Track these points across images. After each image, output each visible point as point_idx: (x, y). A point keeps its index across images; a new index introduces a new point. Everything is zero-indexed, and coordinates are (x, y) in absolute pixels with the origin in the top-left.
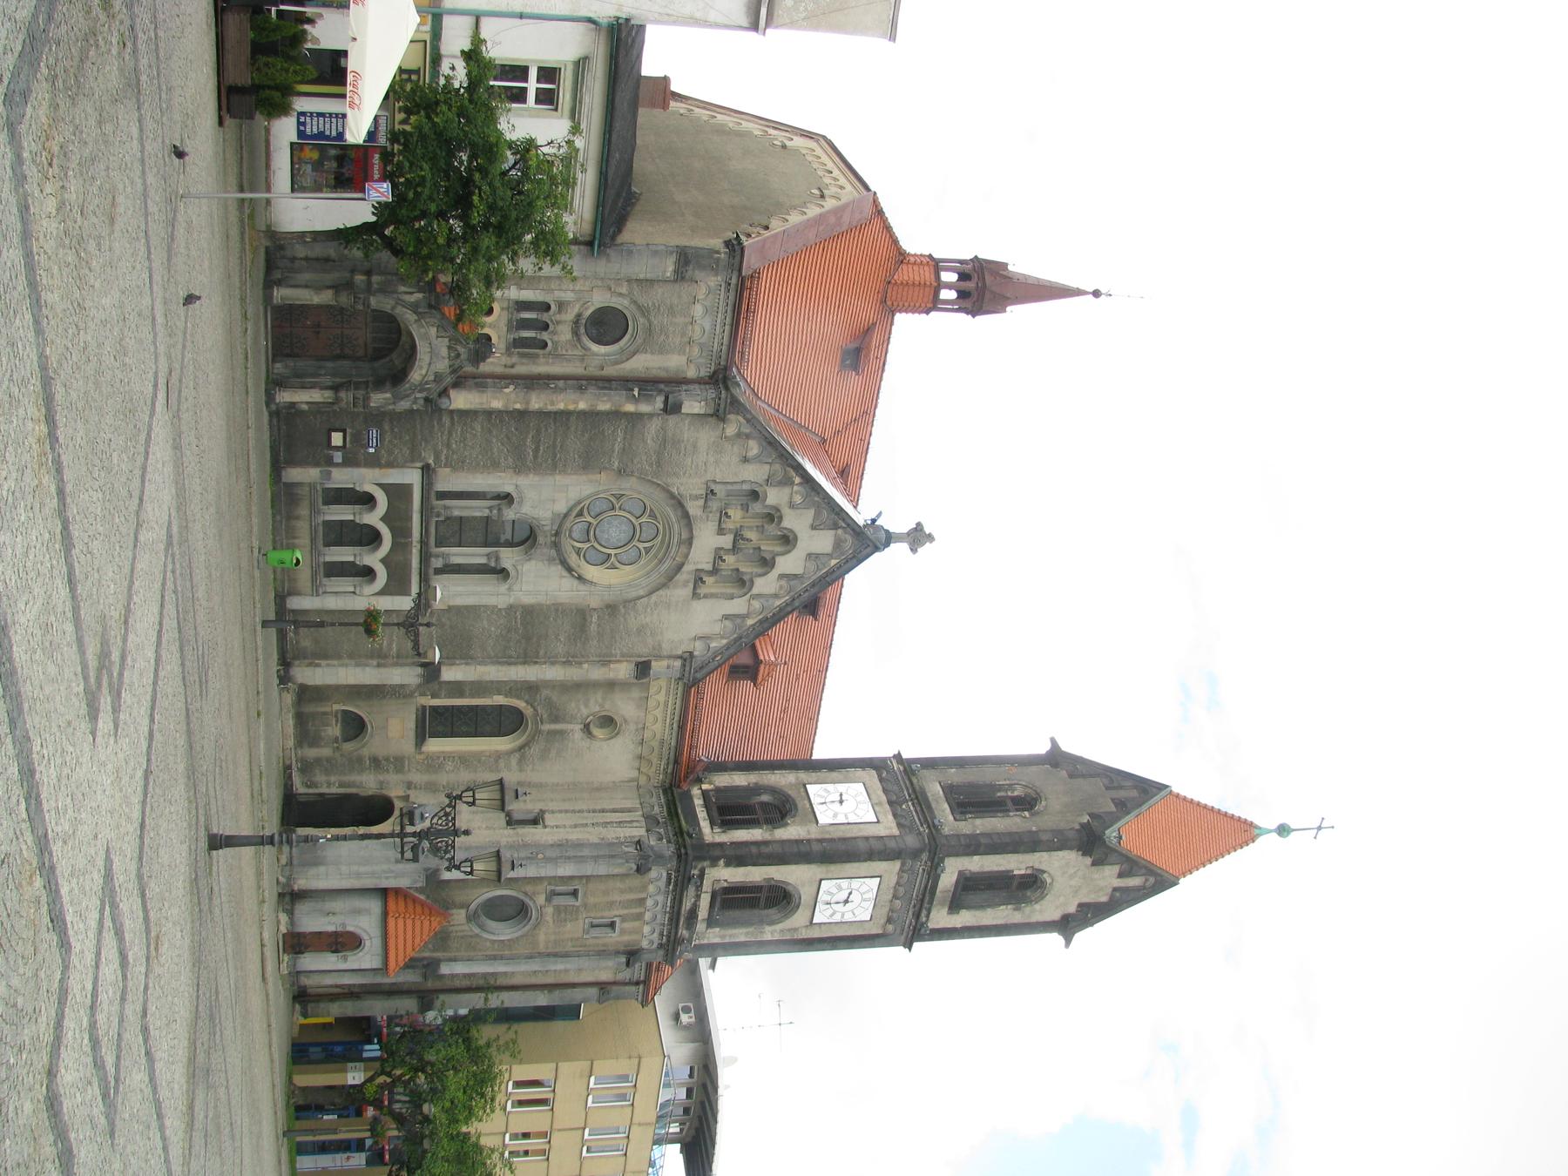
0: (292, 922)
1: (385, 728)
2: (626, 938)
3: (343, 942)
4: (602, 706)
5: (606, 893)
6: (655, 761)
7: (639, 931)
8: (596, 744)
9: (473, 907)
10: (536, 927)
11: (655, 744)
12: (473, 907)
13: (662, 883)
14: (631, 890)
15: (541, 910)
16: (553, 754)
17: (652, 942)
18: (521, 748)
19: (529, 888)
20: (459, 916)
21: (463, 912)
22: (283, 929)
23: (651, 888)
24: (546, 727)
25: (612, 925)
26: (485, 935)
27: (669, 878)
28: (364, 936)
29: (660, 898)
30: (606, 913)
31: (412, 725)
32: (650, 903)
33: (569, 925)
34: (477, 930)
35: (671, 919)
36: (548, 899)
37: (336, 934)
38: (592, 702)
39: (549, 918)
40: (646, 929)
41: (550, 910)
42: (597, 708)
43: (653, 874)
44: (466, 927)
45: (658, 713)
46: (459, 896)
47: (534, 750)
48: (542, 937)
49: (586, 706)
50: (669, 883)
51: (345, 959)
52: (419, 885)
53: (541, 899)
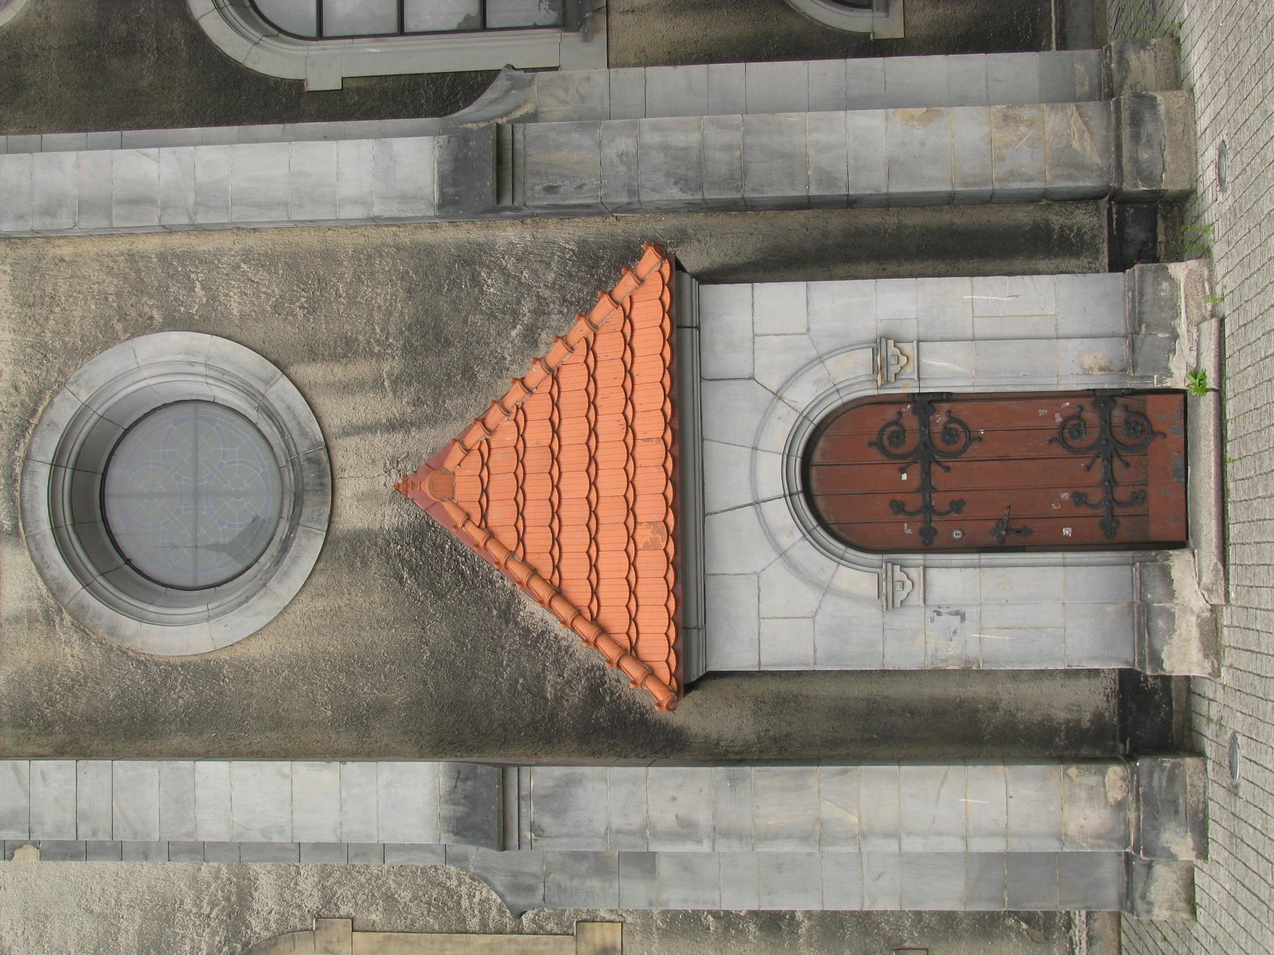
0: (1144, 620)
3: (895, 474)
12: (309, 548)
19: (70, 653)
20: (365, 497)
21: (353, 516)
22: (1190, 576)
28: (779, 514)
34: (283, 393)
37: (929, 543)
44: (338, 411)
46: (370, 614)
51: (883, 347)
52: (540, 778)
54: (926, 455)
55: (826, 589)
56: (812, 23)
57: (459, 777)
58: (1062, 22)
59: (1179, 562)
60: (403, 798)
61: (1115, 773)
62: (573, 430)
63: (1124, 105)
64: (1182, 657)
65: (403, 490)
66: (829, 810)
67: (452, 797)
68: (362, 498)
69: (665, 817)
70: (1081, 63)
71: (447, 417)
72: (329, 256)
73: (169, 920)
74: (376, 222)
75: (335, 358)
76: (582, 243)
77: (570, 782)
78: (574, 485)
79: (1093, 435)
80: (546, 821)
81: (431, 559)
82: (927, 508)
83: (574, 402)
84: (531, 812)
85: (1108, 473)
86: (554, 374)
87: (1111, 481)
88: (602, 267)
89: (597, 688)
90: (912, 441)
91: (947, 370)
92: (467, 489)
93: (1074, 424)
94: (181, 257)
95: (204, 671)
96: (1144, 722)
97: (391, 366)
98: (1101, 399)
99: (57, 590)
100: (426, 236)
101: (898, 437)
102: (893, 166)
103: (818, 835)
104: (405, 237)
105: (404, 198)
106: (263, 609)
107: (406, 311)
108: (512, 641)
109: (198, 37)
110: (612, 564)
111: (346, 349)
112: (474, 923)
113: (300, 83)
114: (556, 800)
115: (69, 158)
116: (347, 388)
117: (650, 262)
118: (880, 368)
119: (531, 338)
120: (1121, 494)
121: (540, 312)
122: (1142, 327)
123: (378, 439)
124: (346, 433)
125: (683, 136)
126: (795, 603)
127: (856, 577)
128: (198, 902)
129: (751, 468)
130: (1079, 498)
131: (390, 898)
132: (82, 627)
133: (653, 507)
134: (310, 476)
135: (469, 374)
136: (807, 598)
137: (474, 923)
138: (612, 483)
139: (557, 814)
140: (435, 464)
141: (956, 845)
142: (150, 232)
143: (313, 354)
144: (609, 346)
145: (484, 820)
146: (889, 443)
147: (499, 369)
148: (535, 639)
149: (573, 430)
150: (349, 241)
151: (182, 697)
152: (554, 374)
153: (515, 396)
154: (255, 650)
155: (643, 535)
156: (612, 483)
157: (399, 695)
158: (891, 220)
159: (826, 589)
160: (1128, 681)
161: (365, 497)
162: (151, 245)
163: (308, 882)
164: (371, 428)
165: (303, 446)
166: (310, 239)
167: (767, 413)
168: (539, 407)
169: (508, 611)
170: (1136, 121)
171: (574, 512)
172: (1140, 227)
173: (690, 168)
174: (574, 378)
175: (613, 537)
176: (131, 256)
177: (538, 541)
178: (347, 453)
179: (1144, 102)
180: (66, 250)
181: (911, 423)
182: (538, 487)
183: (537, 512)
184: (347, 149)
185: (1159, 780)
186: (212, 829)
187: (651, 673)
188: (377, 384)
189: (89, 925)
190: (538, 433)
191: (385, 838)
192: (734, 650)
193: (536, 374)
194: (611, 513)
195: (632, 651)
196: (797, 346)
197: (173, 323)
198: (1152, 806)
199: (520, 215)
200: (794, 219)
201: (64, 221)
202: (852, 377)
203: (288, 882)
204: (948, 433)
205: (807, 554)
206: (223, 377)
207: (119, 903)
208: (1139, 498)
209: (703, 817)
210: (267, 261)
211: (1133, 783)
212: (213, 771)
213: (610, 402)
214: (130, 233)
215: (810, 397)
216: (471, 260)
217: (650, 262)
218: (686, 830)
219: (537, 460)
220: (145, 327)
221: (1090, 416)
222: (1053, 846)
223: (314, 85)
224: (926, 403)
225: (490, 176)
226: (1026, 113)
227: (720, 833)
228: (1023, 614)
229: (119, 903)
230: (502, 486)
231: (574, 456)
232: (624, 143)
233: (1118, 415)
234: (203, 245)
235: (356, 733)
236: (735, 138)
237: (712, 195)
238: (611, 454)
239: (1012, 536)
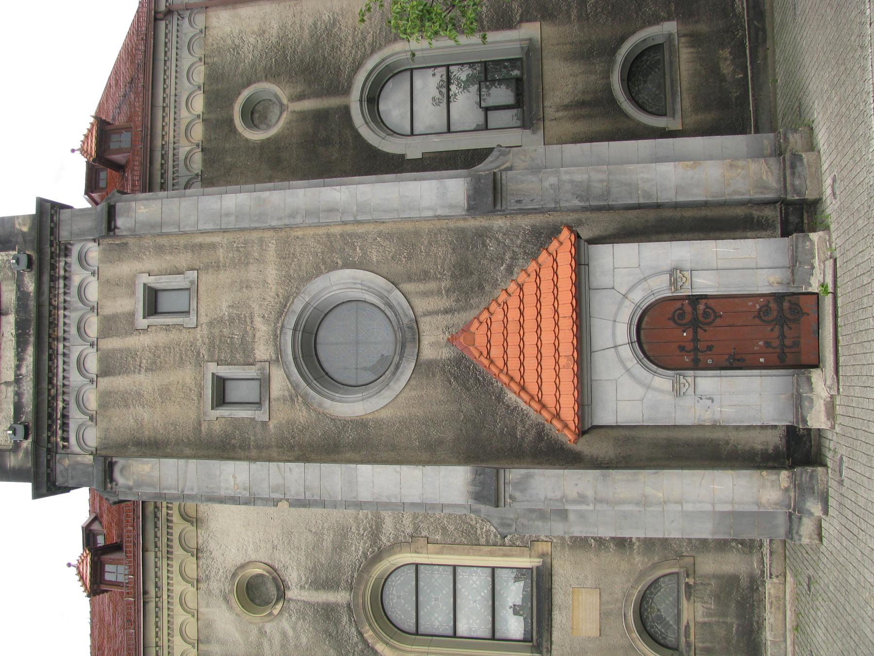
0: (799, 402)
1: (604, 615)
2: (124, 269)
3: (681, 333)
4: (262, 633)
5: (165, 393)
6: (176, 518)
7: (108, 285)
8: (263, 556)
9: (408, 368)
10: (282, 311)
11: (178, 551)
12: (408, 368)
13: (76, 417)
14: (126, 399)
15: (278, 359)
16: (327, 543)
17: (82, 260)
18: (377, 557)
19: (301, 415)
20: (433, 345)
21: (428, 353)
22: (820, 382)
23: (92, 401)
24: (341, 597)
25: (153, 302)
26: (380, 281)
27: (65, 426)
28: (626, 352)
29: (75, 378)
30: (162, 338)
31: (558, 618)
32: (92, 365)
33: (224, 307)
34: (396, 297)
35: (53, 325)
36: (264, 382)
37: (697, 365)
38: (277, 639)
39: (262, 329)
40: (93, 293)
41: (263, 351)
42: (268, 627)
43: (92, 437)
44: (421, 305)
45: (180, 616)
47: (358, 549)
48: (272, 273)
49: (284, 634)
50: (65, 416)
51: (675, 273)
52: (514, 474)
53: (278, 384)
54: (695, 324)
55: (648, 387)
56: (639, 123)
57: (476, 473)
58: (756, 121)
59: (815, 374)
60: (452, 483)
61: (784, 474)
62: (530, 313)
63: (787, 159)
64: (817, 419)
65: (451, 341)
66: (649, 491)
67: (473, 483)
68: (432, 345)
69: (572, 493)
70: (766, 140)
71: (471, 307)
72: (417, 234)
73: (345, 536)
74: (439, 218)
75: (420, 280)
76: (533, 227)
77: (528, 477)
78: (530, 339)
79: (774, 314)
80: (517, 494)
81: (464, 373)
82: (696, 349)
83: (530, 300)
84: (510, 490)
85: (783, 333)
86: (521, 287)
87: (783, 336)
88: (542, 238)
89: (541, 433)
90: (688, 318)
91: (705, 284)
92: (481, 340)
93: (765, 310)
94: (350, 235)
95: (361, 423)
96: (798, 450)
97: (446, 283)
98: (778, 297)
99: (296, 387)
100: (461, 224)
101: (682, 315)
102: (678, 189)
103: (644, 502)
104: (452, 224)
105: (451, 207)
106: (387, 396)
107: (452, 258)
108: (501, 411)
109: (357, 136)
110: (548, 375)
111: (425, 276)
112: (483, 541)
113: (403, 156)
114: (522, 485)
115: (301, 192)
116: (425, 294)
117: (565, 234)
118: (673, 283)
119: (510, 270)
120: (788, 342)
121: (514, 258)
122: (797, 263)
123: (440, 317)
124: (425, 315)
125: (580, 176)
126: (634, 392)
127: (662, 381)
128: (358, 529)
129: (613, 330)
130: (768, 344)
131: (444, 529)
132: (307, 403)
133: (567, 348)
134: (409, 335)
135: (481, 287)
136: (639, 391)
137: (483, 541)
138: (548, 338)
139: (523, 491)
140: (466, 329)
141: (708, 507)
142: (337, 224)
143: (410, 279)
144: (546, 274)
145: (488, 493)
146: (677, 318)
147: (495, 285)
148: (512, 410)
149: (530, 313)
150: (426, 226)
151: (350, 435)
152: (521, 287)
153: (503, 297)
154: (384, 414)
155: (563, 361)
156: (548, 338)
157: (449, 436)
158: (677, 214)
159: (648, 387)
160: (791, 431)
161: (433, 345)
162: (337, 230)
163: (407, 521)
164: (436, 313)
165: (406, 321)
166: (409, 226)
167: (620, 304)
168: (514, 302)
169: (500, 397)
170: (793, 166)
171: (530, 351)
172: (794, 216)
173: (584, 191)
174: (530, 289)
175: (548, 363)
176: (328, 235)
177: (514, 364)
178: (425, 324)
179: (796, 158)
180: (299, 233)
181: (688, 309)
182: (513, 339)
183: (513, 351)
184: (425, 184)
185: (805, 478)
186: (365, 495)
187: (566, 426)
188: (439, 292)
189: (310, 537)
190: (513, 314)
191: (443, 501)
192: (605, 416)
193: (512, 287)
194: (548, 351)
195: (557, 416)
196: (634, 274)
197: (347, 265)
198: (803, 490)
199: (505, 214)
200: (632, 214)
201: (299, 220)
202: (660, 287)
203: (398, 521)
204: (705, 314)
205: (639, 371)
206: (369, 289)
207: (323, 528)
208: (796, 344)
209: (590, 493)
210: (389, 236)
211: (793, 479)
212: (365, 469)
213: (547, 299)
214: (328, 225)
215: (640, 297)
216: (482, 234)
217: (565, 234)
218: (582, 499)
219: (513, 327)
220: (334, 267)
221: (773, 305)
222: (755, 508)
223: (409, 156)
224: (695, 300)
225: (490, 195)
226: (741, 163)
227: (598, 501)
228: (743, 399)
229: (323, 528)
230: (496, 339)
231: (530, 325)
232: (552, 180)
233: (786, 305)
234: (360, 229)
235: (431, 453)
236: (603, 176)
237: (594, 203)
238: (547, 324)
239: (736, 362)
